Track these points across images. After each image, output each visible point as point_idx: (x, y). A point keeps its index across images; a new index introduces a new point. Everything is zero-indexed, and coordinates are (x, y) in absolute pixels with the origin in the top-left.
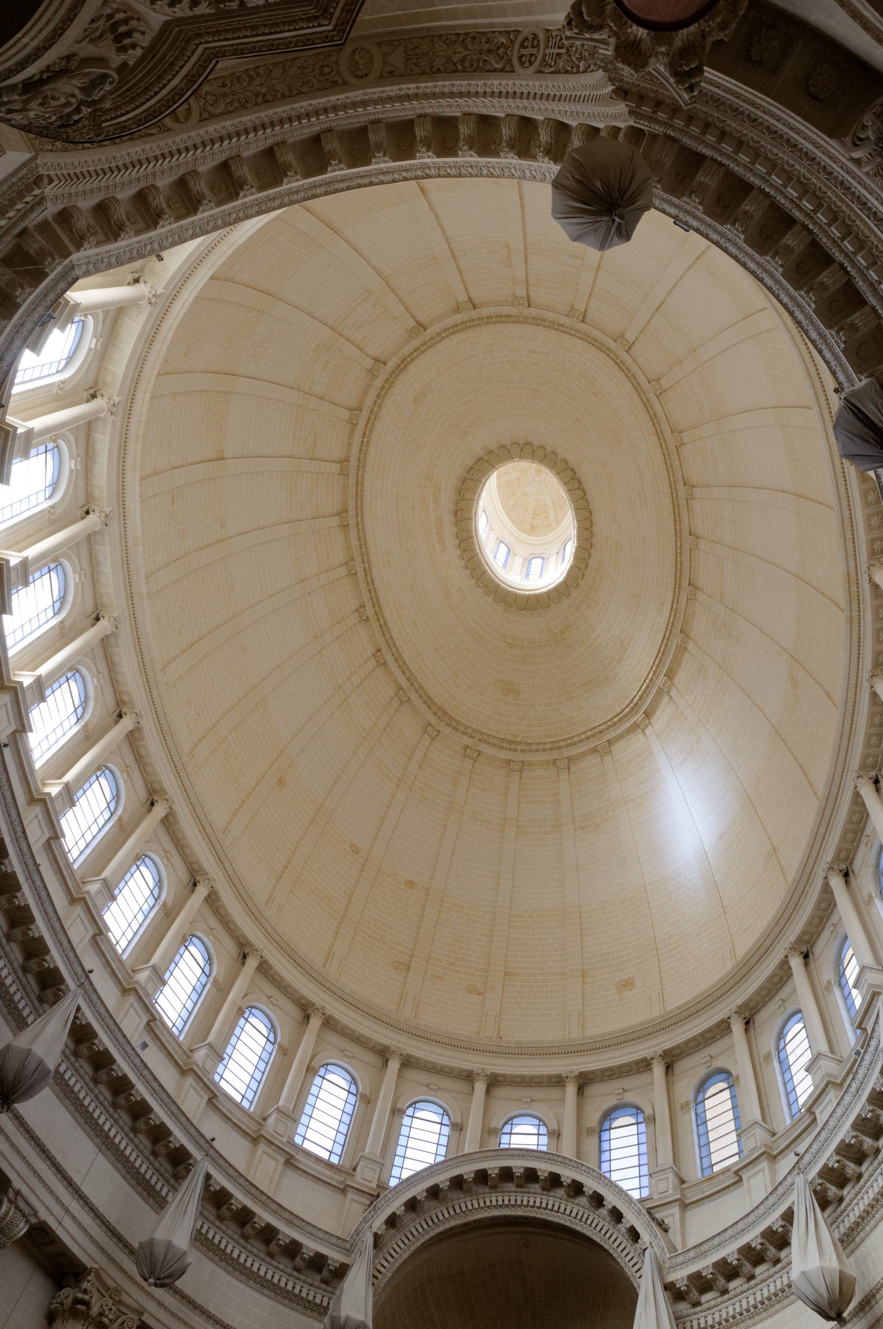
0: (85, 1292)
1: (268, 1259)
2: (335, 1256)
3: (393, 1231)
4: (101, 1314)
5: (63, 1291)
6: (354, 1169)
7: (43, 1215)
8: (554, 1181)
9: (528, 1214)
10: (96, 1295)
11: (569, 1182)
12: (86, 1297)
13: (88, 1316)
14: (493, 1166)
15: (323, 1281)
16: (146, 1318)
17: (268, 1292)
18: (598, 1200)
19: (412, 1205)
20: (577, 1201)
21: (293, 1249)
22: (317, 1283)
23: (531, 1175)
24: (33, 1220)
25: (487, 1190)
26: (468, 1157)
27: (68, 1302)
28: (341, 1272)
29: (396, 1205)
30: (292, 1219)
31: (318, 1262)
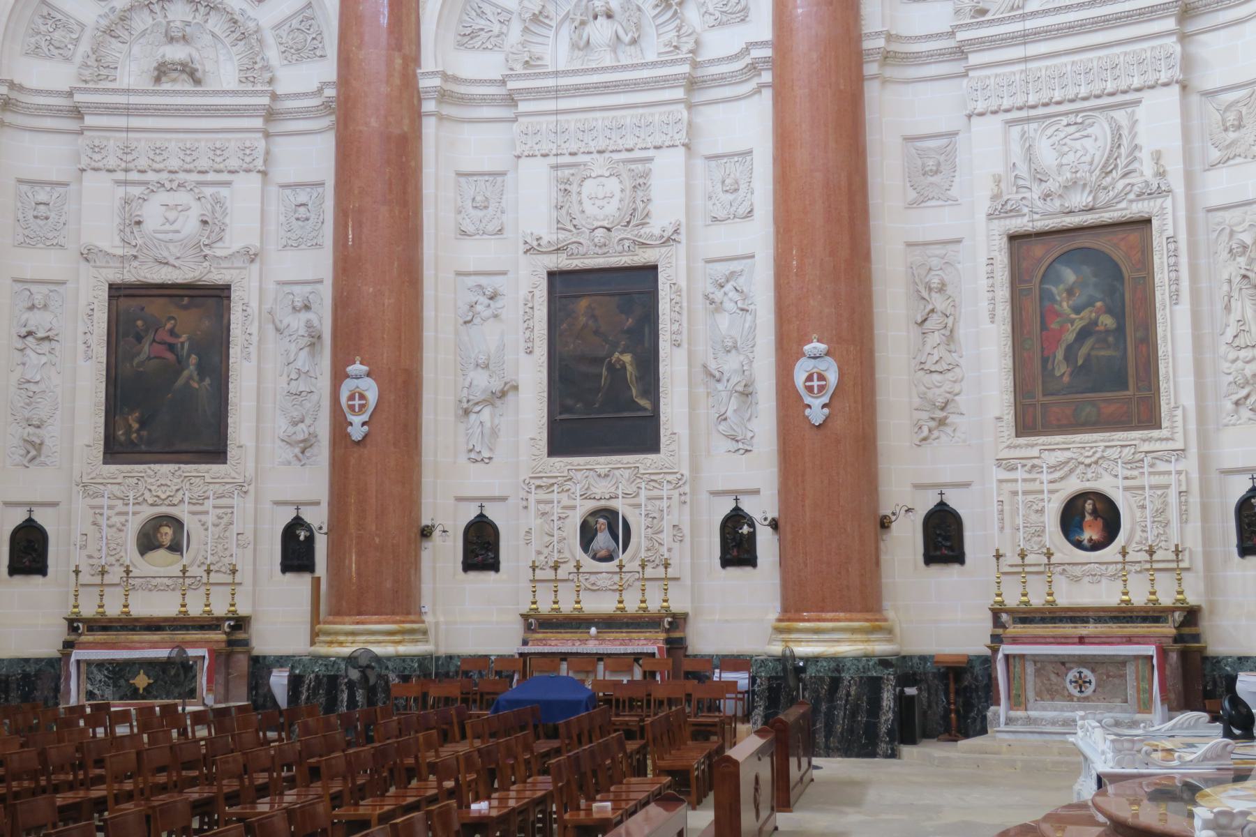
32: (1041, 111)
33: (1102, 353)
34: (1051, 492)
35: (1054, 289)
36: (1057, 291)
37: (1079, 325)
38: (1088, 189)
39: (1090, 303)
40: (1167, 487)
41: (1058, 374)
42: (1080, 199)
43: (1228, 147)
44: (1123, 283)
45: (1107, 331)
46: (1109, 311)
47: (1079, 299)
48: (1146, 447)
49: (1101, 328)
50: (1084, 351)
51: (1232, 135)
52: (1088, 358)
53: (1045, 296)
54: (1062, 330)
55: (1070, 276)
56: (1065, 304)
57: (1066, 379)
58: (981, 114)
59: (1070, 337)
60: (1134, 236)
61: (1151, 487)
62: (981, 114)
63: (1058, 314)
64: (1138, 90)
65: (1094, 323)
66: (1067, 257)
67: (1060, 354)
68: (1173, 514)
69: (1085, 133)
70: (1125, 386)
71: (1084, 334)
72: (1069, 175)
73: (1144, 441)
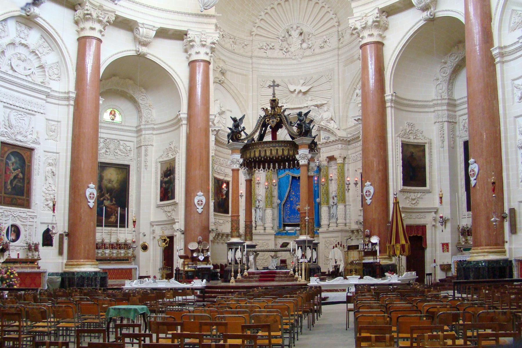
32: (12, 107)
33: (19, 184)
34: (5, 224)
36: (10, 163)
37: (14, 174)
38: (22, 135)
39: (17, 169)
41: (8, 188)
42: (19, 137)
43: (50, 136)
44: (25, 165)
45: (21, 178)
46: (22, 173)
47: (15, 166)
48: (28, 214)
49: (19, 177)
50: (15, 183)
51: (52, 134)
52: (16, 185)
54: (10, 175)
55: (13, 159)
56: (11, 167)
57: (10, 190)
59: (12, 177)
60: (29, 153)
61: (29, 225)
63: (9, 170)
64: (36, 112)
65: (18, 175)
66: (13, 153)
67: (9, 182)
69: (23, 119)
70: (23, 195)
71: (15, 177)
72: (18, 129)
73: (28, 212)
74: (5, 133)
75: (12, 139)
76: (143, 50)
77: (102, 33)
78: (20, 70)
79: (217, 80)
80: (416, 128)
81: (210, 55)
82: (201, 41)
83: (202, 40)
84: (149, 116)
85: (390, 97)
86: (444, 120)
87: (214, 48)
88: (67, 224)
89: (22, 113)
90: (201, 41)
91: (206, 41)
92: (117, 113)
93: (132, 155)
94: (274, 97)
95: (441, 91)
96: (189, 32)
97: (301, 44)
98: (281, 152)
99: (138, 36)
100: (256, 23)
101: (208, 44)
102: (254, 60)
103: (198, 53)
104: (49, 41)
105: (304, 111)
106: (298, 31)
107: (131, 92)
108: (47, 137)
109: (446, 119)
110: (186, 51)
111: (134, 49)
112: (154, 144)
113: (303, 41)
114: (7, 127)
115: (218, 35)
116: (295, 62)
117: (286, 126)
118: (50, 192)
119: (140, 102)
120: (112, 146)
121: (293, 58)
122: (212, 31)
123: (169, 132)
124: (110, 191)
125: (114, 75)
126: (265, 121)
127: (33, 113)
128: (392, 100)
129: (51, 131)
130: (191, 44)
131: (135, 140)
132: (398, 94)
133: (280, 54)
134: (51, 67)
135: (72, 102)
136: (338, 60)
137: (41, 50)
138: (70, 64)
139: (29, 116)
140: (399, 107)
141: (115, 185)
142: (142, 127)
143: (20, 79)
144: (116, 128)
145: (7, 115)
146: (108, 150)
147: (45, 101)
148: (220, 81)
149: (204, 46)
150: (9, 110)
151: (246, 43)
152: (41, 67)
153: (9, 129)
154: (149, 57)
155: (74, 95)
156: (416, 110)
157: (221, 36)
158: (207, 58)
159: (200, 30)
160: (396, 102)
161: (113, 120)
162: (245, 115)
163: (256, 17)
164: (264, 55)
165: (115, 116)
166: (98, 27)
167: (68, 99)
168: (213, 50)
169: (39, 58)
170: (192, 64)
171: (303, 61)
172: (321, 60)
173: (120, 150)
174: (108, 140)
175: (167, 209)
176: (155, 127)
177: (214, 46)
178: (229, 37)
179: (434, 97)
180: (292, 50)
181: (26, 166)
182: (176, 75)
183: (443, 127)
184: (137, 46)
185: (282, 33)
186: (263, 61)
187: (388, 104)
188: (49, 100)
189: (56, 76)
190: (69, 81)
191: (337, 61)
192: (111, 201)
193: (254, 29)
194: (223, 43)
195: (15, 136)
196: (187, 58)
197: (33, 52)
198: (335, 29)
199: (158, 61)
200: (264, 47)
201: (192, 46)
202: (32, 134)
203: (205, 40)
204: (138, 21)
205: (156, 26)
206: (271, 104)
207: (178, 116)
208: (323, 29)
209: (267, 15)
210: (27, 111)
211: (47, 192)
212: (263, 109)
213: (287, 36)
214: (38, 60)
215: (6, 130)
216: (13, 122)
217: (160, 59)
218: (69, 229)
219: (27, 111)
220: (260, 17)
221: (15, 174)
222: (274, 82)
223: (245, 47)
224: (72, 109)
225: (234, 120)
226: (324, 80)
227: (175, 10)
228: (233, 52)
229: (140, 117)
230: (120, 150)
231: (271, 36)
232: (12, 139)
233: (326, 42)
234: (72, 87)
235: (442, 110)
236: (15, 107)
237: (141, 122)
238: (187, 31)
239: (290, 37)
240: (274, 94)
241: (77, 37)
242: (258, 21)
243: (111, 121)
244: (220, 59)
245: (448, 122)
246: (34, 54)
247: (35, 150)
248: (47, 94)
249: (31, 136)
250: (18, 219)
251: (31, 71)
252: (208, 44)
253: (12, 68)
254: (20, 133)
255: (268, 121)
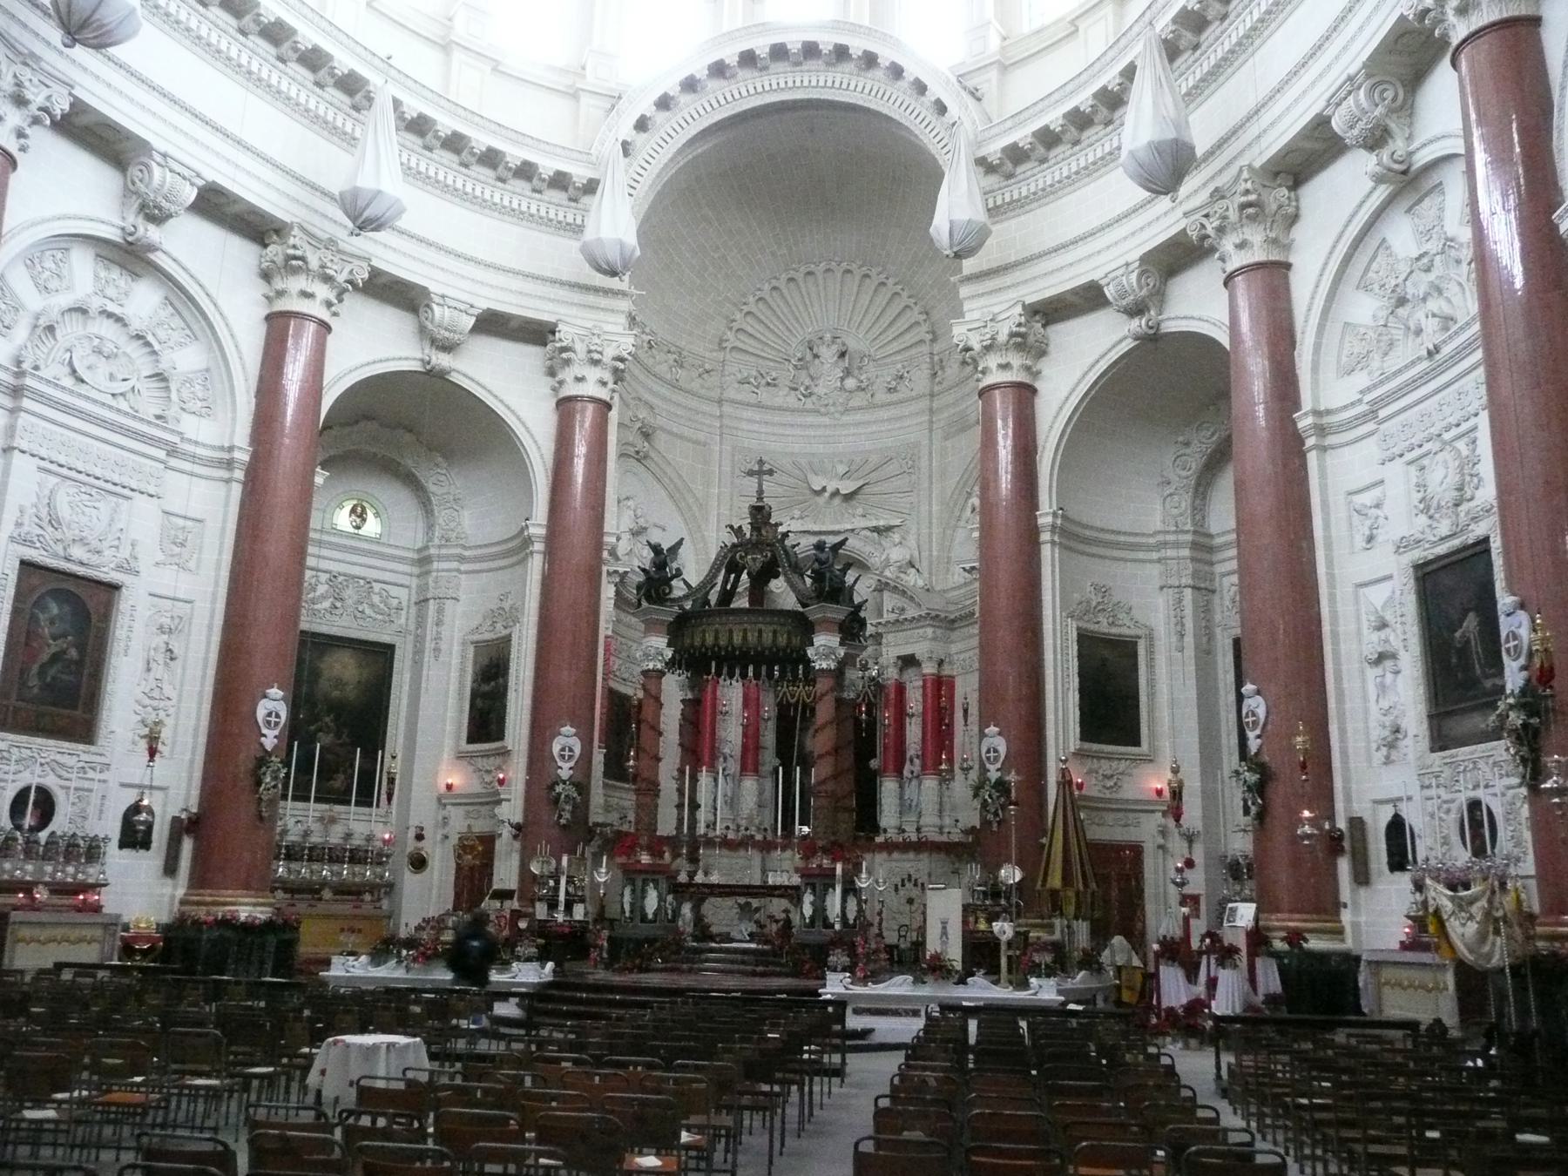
0: (294, 247)
1: (499, 184)
2: (580, 173)
3: (644, 136)
4: (323, 267)
5: (269, 249)
6: (584, 68)
7: (211, 176)
8: (841, 53)
9: (810, 96)
10: (307, 247)
11: (860, 53)
12: (298, 253)
13: (308, 270)
14: (761, 46)
15: (570, 199)
16: (374, 263)
17: (510, 219)
18: (897, 72)
19: (664, 103)
20: (870, 74)
21: (526, 171)
22: (566, 203)
23: (811, 50)
24: (200, 183)
25: (756, 74)
26: (730, 36)
27: (280, 260)
28: (591, 187)
29: (646, 106)
30: (520, 137)
31: (560, 181)
32: (64, 471)
33: (64, 677)
34: (13, 781)
35: (41, 616)
37: (53, 650)
39: (64, 635)
40: (90, 790)
42: (77, 552)
45: (71, 661)
47: (59, 627)
48: (84, 757)
50: (52, 672)
51: (177, 550)
52: (53, 678)
53: (33, 619)
55: (54, 609)
57: (36, 690)
58: (23, 452)
59: (45, 657)
62: (23, 452)
64: (133, 490)
65: (64, 652)
66: (57, 594)
67: (35, 668)
68: (92, 811)
69: (96, 505)
70: (75, 708)
71: (55, 658)
72: (77, 532)
74: (35, 539)
75: (56, 556)
76: (442, 360)
77: (333, 309)
78: (98, 376)
79: (631, 450)
80: (1115, 600)
81: (611, 385)
82: (590, 351)
83: (593, 348)
84: (452, 525)
85: (1049, 519)
86: (1184, 581)
87: (623, 371)
88: (195, 793)
89: (94, 491)
90: (590, 351)
91: (601, 353)
92: (370, 515)
93: (403, 621)
94: (760, 499)
95: (1175, 511)
96: (560, 327)
97: (842, 379)
98: (769, 635)
99: (430, 326)
100: (734, 321)
101: (607, 358)
102: (727, 409)
103: (579, 380)
104: (186, 313)
105: (831, 540)
106: (835, 348)
107: (409, 462)
108: (160, 557)
109: (1190, 582)
110: (552, 373)
111: (419, 355)
112: (463, 597)
113: (848, 372)
114: (45, 524)
115: (631, 340)
116: (826, 420)
117: (785, 575)
118: (155, 703)
119: (432, 488)
120: (350, 594)
121: (823, 410)
122: (620, 329)
123: (501, 568)
124: (337, 708)
125: (368, 417)
126: (733, 557)
127: (126, 492)
128: (1054, 527)
129: (175, 543)
130: (564, 355)
131: (414, 582)
132: (1070, 514)
133: (791, 400)
134: (188, 381)
135: (239, 474)
136: (931, 422)
137: (162, 334)
138: (242, 378)
139: (114, 499)
140: (1072, 544)
141: (351, 693)
142: (432, 551)
143: (95, 401)
144: (364, 550)
145: (47, 492)
146: (338, 604)
147: (162, 466)
148: (638, 452)
149: (596, 363)
150: (54, 480)
151: (707, 366)
152: (160, 377)
153: (50, 529)
154: (455, 378)
155: (246, 458)
156: (1116, 553)
157: (645, 345)
158: (603, 394)
159: (589, 325)
160: (1063, 532)
161: (358, 527)
162: (682, 539)
163: (735, 305)
164: (752, 399)
165: (364, 520)
166: (323, 291)
167: (229, 464)
168: (618, 375)
169: (154, 353)
170: (566, 406)
171: (846, 419)
172: (889, 420)
173: (372, 606)
174: (341, 579)
175: (481, 763)
176: (467, 553)
177: (621, 366)
178: (666, 349)
179: (1159, 526)
180: (820, 390)
181: (93, 631)
182: (523, 429)
183: (1180, 601)
184: (427, 351)
185: (797, 350)
186: (748, 414)
187: (1045, 536)
188: (173, 462)
189: (199, 404)
190: (234, 419)
191: (926, 425)
192: (338, 735)
193: (730, 335)
194: (650, 362)
195: (65, 549)
196: (554, 389)
197: (138, 337)
198: (925, 349)
199: (480, 389)
200: (752, 380)
201: (568, 362)
202: (117, 547)
203: (599, 349)
204: (432, 287)
205: (476, 304)
206: (752, 515)
207: (522, 530)
208: (895, 346)
209: (761, 304)
210: (109, 487)
211: (147, 702)
212: (731, 527)
213: (809, 357)
214: (154, 358)
215: (40, 532)
216: (64, 511)
217: (484, 387)
218: (200, 805)
219: (109, 487)
220: (746, 308)
221: (57, 649)
222: (761, 462)
223: (705, 376)
224: (237, 490)
225: (656, 549)
226: (892, 468)
227: (527, 270)
228: (674, 385)
229: (430, 527)
230: (372, 606)
231: (770, 354)
232: (56, 556)
233: (901, 377)
234: (241, 435)
235: (1178, 558)
236: (73, 474)
237: (430, 540)
238: (556, 325)
239: (817, 361)
240: (760, 492)
241: (267, 312)
242: (738, 316)
243: (352, 530)
244: (640, 400)
245: (1194, 587)
246: (141, 342)
247: (124, 590)
248: (169, 448)
249: (113, 551)
250: (53, 770)
251: (128, 385)
252: (607, 358)
253: (74, 371)
254: (82, 541)
255: (741, 557)
